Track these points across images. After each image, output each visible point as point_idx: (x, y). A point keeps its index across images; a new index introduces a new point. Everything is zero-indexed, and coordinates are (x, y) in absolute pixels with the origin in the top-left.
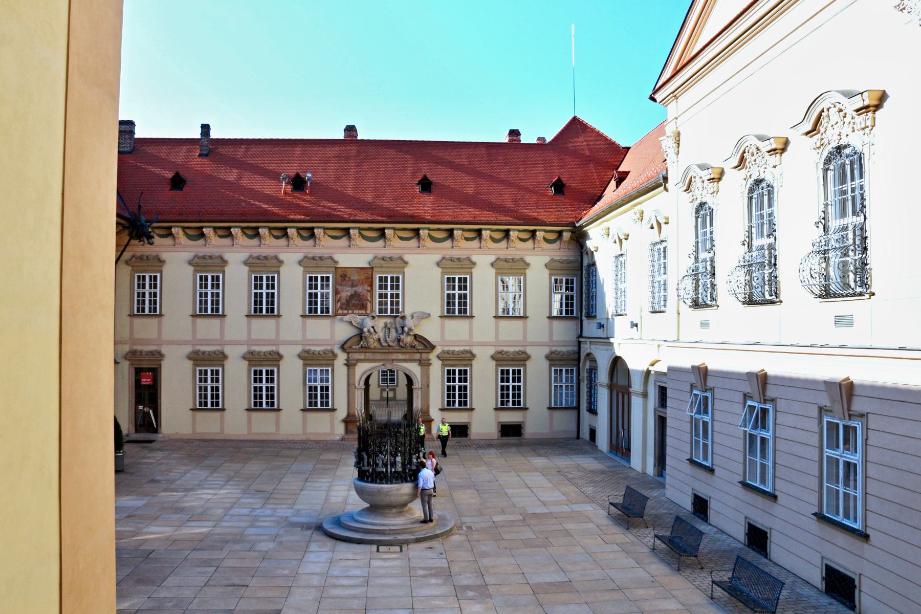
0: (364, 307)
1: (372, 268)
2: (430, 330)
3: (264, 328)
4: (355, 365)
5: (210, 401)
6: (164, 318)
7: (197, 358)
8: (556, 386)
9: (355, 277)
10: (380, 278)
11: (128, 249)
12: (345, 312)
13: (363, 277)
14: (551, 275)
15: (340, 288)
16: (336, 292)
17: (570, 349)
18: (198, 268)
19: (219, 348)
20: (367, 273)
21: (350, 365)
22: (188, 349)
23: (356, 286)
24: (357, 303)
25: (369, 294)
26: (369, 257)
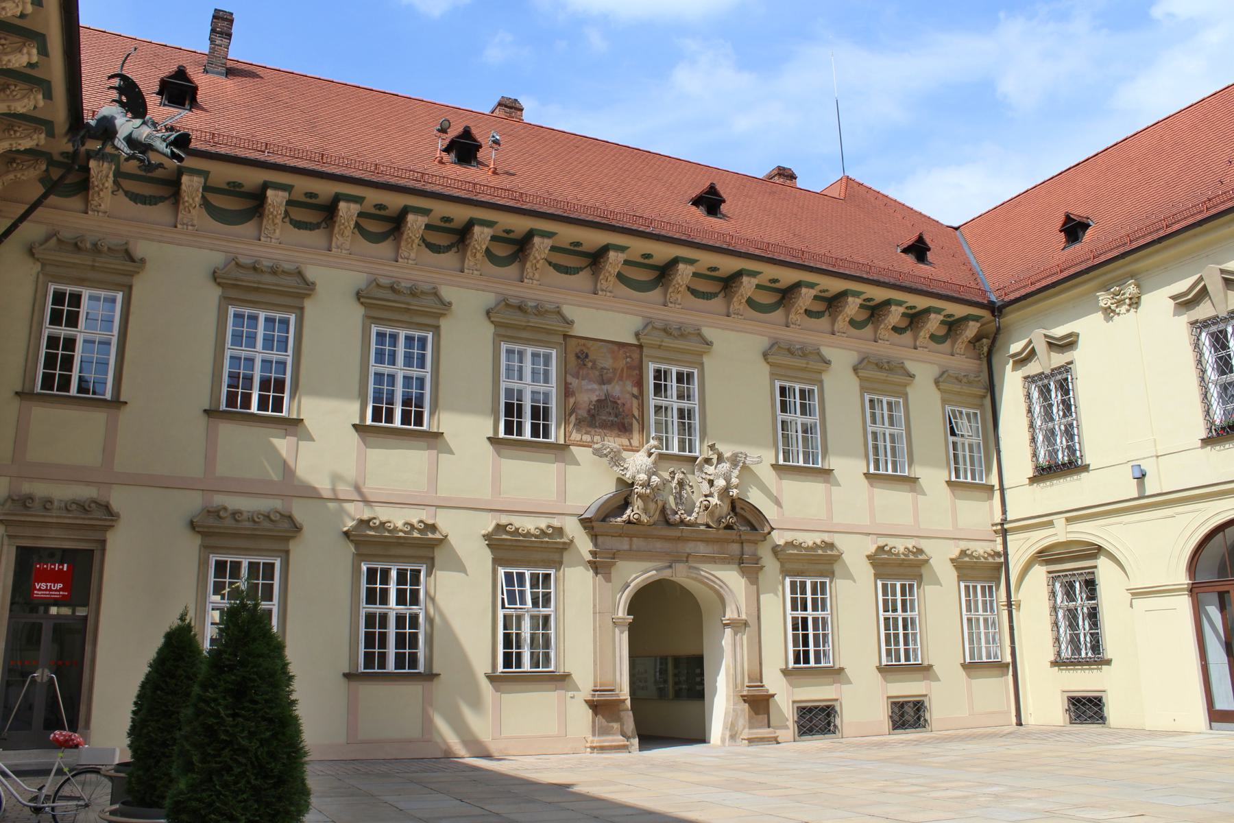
1: (640, 347)
6: (125, 415)
7: (211, 528)
8: (970, 620)
9: (606, 362)
11: (39, 212)
13: (621, 364)
15: (575, 383)
18: (233, 293)
19: (277, 504)
20: (631, 355)
22: (193, 503)
23: (609, 381)
24: (611, 418)
26: (636, 323)
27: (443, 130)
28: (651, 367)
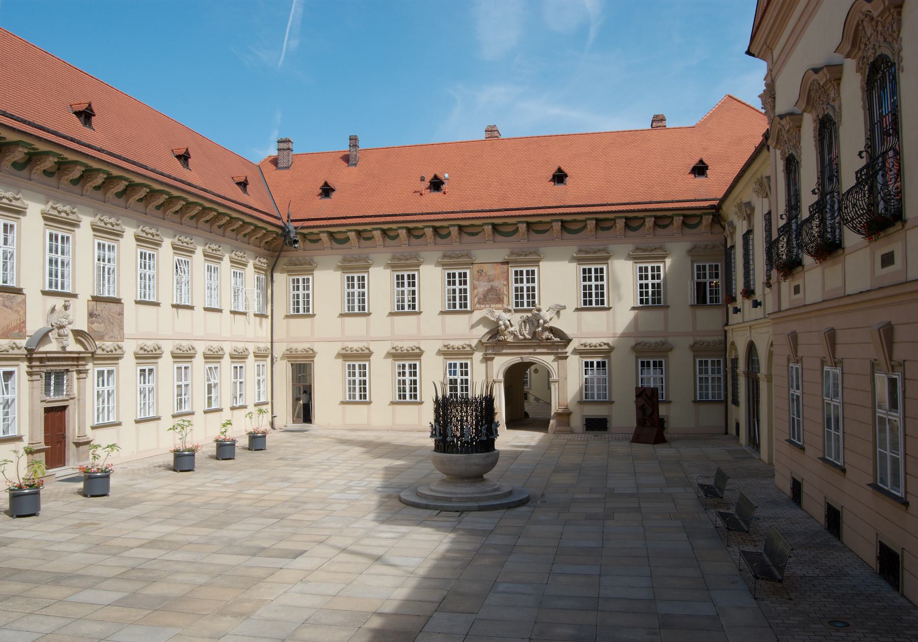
0: (500, 300)
2: (566, 323)
3: (406, 323)
4: (492, 359)
5: (360, 394)
10: (516, 272)
12: (483, 306)
14: (693, 262)
15: (475, 282)
16: (474, 288)
17: (716, 338)
21: (487, 359)
23: (493, 280)
25: (505, 288)
27: (422, 179)
28: (514, 269)
